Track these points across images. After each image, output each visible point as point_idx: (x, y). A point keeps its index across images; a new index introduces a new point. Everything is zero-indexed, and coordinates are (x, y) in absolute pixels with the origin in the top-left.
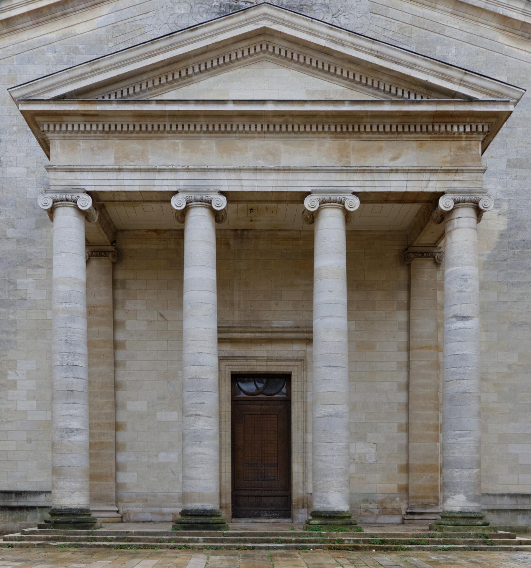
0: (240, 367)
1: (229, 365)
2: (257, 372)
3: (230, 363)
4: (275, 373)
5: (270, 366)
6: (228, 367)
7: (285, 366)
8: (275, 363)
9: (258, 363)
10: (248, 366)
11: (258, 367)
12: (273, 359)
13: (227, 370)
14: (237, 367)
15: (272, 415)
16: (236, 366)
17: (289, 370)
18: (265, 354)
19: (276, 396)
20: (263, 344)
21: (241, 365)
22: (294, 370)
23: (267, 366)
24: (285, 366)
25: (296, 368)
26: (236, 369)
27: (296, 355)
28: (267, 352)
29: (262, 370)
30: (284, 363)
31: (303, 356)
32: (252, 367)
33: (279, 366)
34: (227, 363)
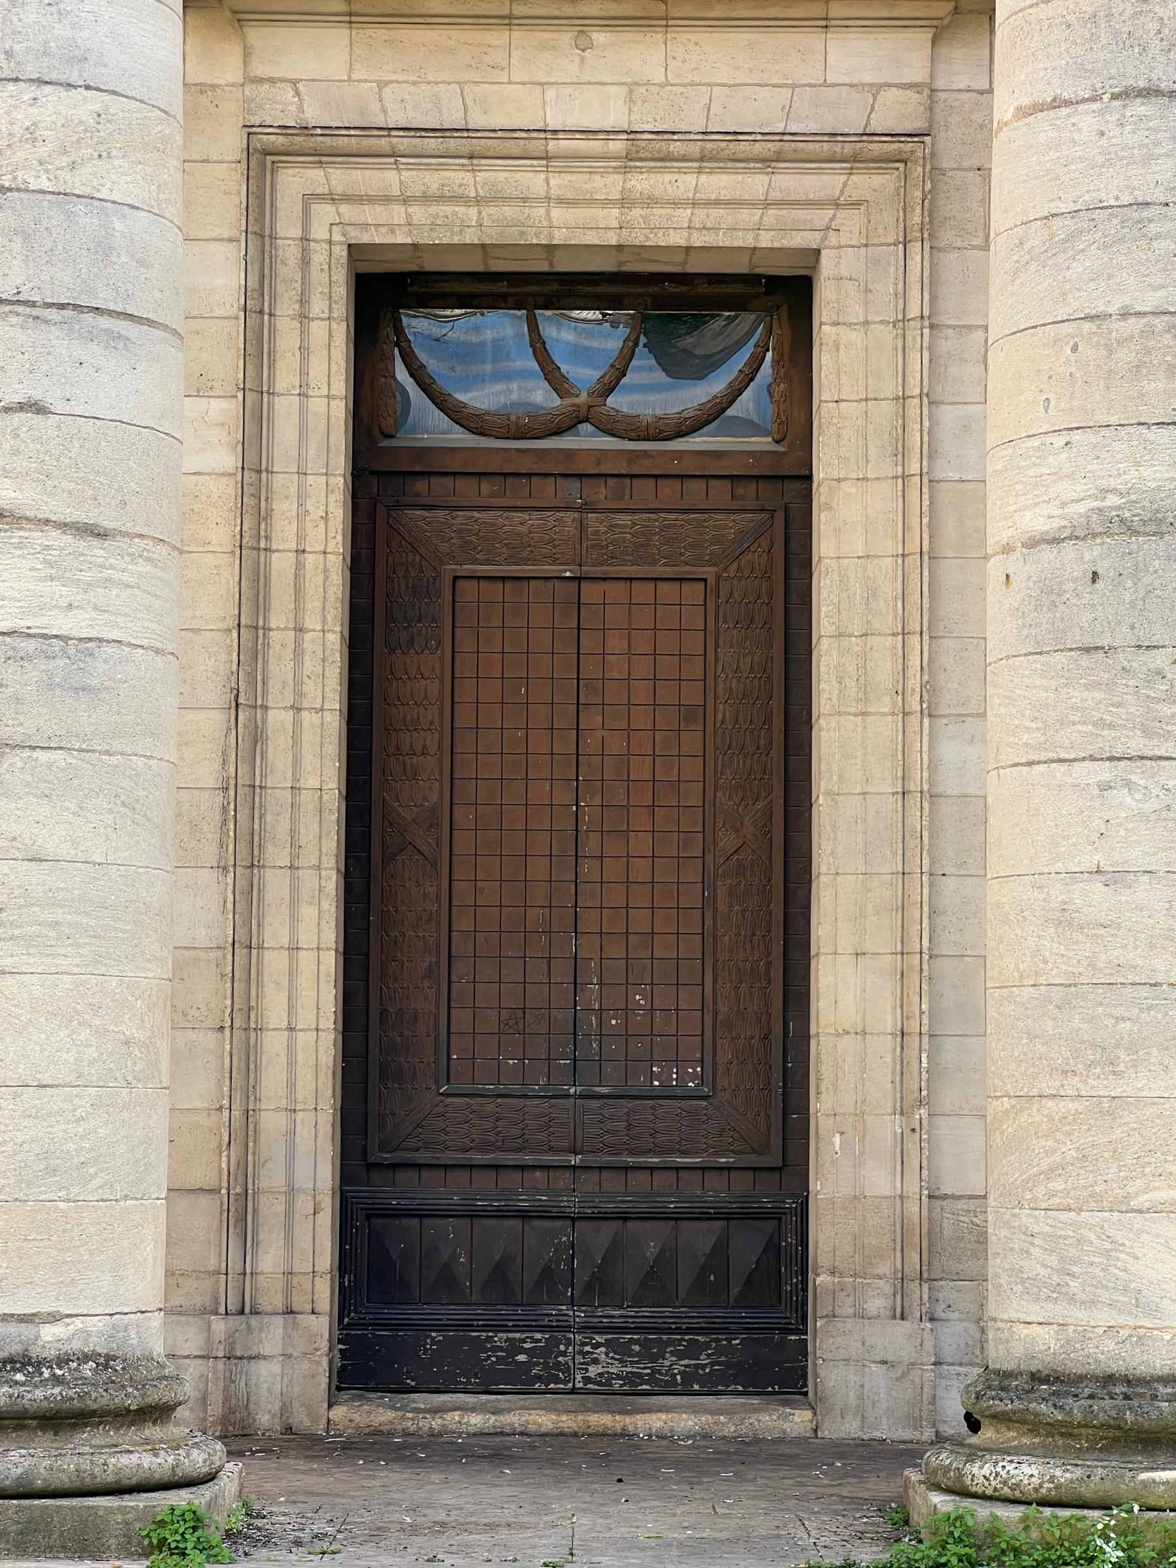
0: (418, 213)
1: (332, 198)
2: (550, 248)
3: (340, 177)
4: (695, 266)
5: (651, 202)
6: (324, 213)
7: (767, 204)
8: (684, 183)
9: (560, 183)
10: (478, 201)
11: (557, 213)
12: (676, 148)
13: (319, 232)
14: (398, 213)
15: (663, 587)
16: (387, 200)
17: (798, 240)
18: (615, 115)
19: (698, 442)
20: (600, 37)
21: (425, 199)
22: (833, 239)
23: (625, 201)
24: (767, 204)
25: (850, 223)
26: (392, 228)
27: (852, 119)
28: (630, 99)
29: (591, 238)
30: (756, 184)
31: (908, 127)
32: (509, 211)
33: (717, 203)
34: (313, 177)
